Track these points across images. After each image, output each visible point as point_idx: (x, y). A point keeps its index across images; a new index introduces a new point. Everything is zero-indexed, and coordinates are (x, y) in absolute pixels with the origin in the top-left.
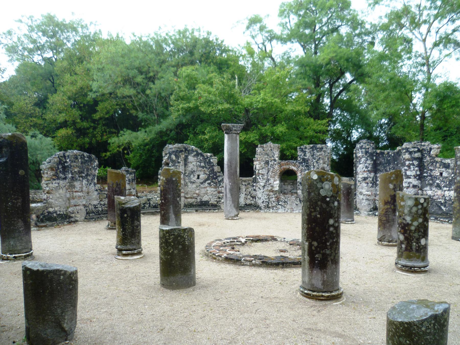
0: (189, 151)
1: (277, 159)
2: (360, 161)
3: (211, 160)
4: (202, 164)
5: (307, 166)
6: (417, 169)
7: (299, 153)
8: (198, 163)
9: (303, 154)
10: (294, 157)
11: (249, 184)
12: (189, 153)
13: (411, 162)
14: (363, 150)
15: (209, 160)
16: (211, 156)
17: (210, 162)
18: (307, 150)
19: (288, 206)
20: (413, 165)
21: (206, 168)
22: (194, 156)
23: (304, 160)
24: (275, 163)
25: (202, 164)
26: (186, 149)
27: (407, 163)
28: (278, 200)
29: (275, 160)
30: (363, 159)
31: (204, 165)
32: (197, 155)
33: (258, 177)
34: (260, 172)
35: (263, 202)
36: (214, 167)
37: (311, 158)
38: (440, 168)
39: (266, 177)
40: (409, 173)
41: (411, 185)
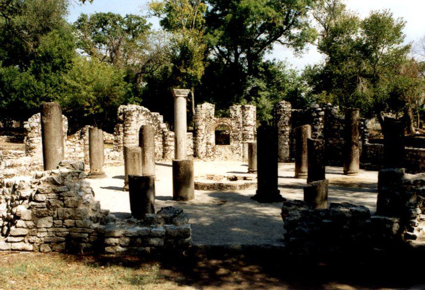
0: (139, 110)
1: (213, 116)
2: (280, 118)
3: (158, 119)
4: (151, 122)
5: (237, 123)
6: (321, 124)
7: (232, 112)
8: (147, 121)
9: (234, 113)
10: (228, 116)
11: (189, 138)
12: (139, 113)
13: (317, 119)
14: (282, 109)
15: (157, 118)
16: (157, 115)
17: (157, 120)
18: (236, 109)
19: (222, 156)
20: (319, 121)
21: (154, 125)
22: (144, 115)
23: (235, 117)
24: (211, 120)
25: (151, 122)
26: (137, 109)
27: (315, 119)
28: (213, 150)
29: (211, 118)
30: (281, 117)
31: (152, 123)
32: (147, 113)
33: (197, 132)
34: (199, 127)
35: (202, 153)
36: (161, 124)
37: (241, 116)
38: (337, 123)
39: (203, 132)
40: (315, 127)
41: (318, 136)
